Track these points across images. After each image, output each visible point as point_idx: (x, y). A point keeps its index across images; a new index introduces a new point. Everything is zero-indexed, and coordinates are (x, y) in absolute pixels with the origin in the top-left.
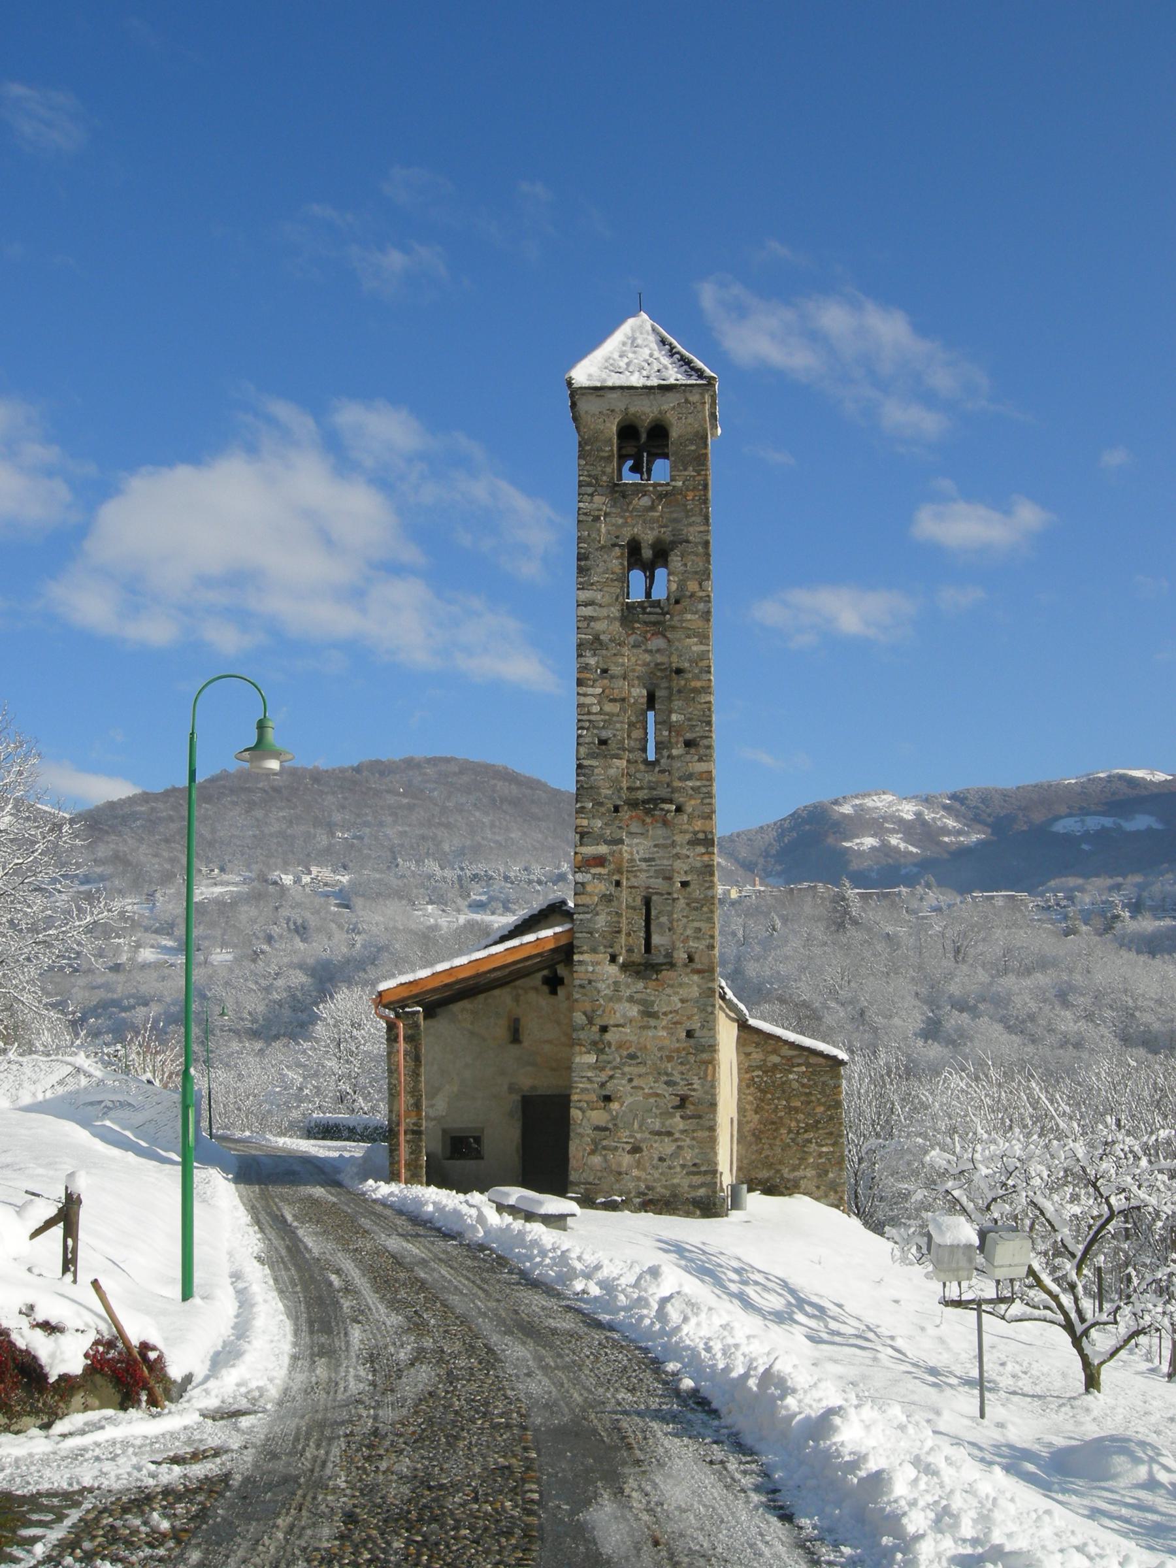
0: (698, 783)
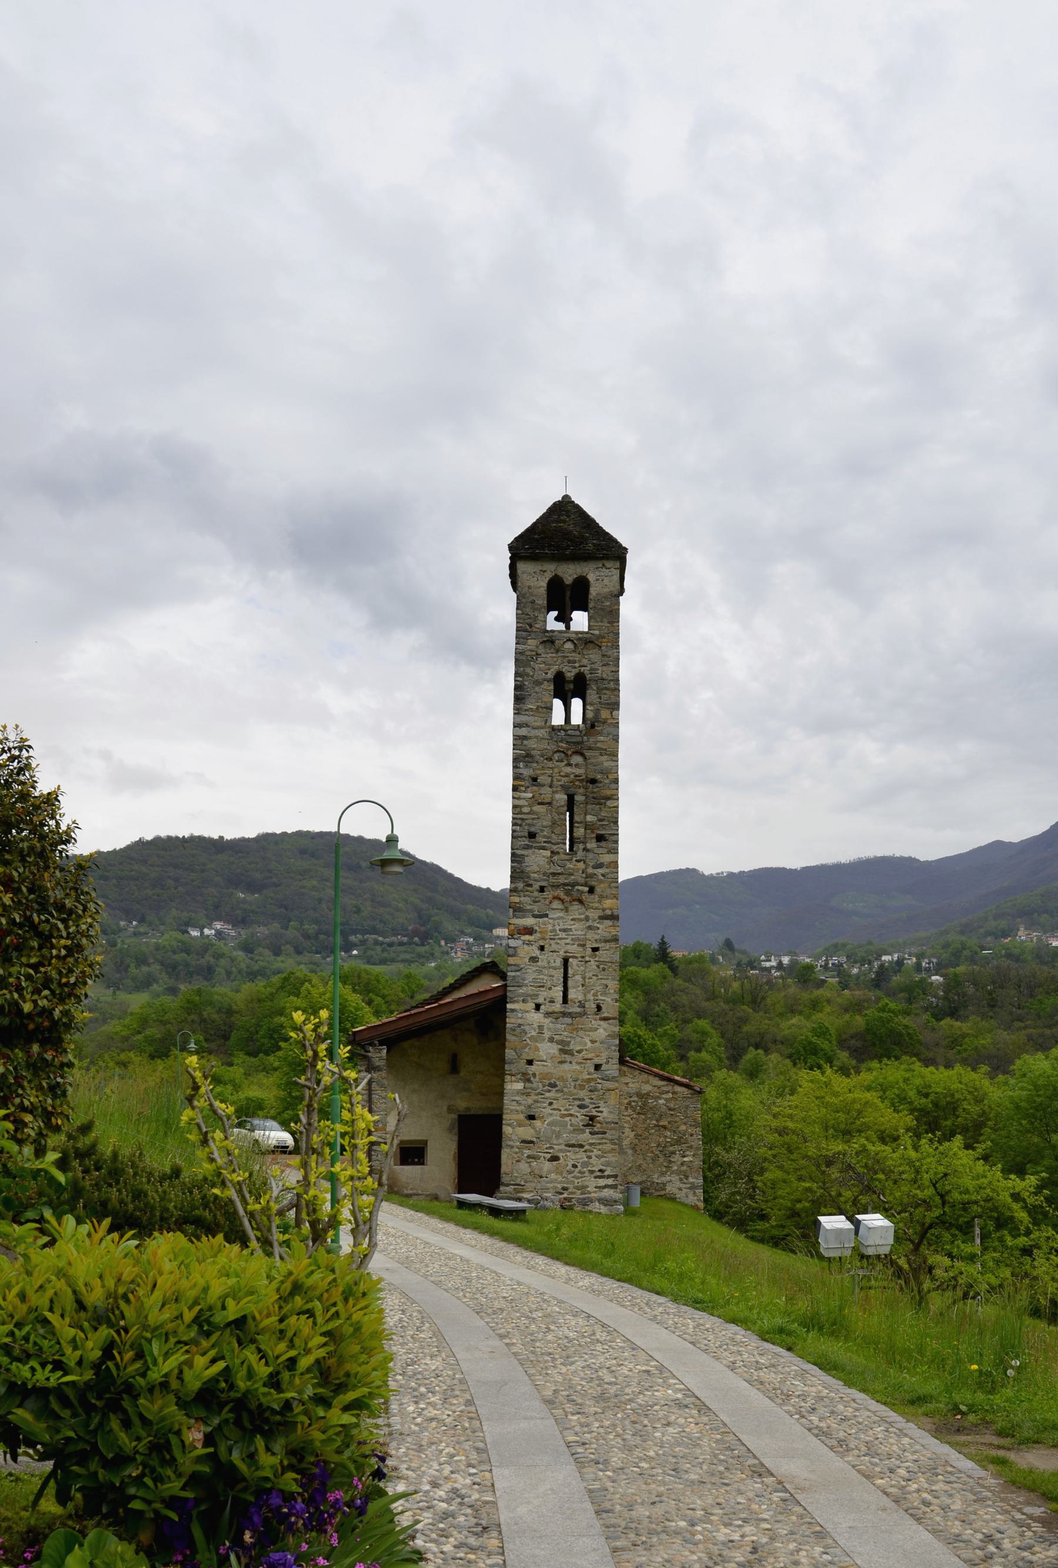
0: (607, 870)
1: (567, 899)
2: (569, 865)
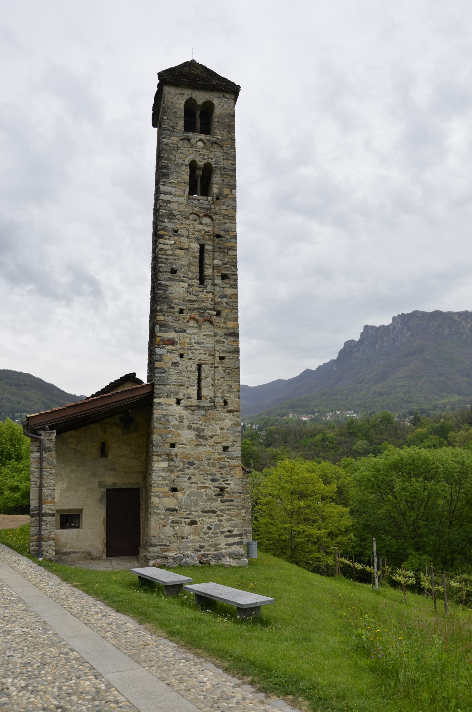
0: (230, 300)
1: (201, 319)
2: (201, 295)
